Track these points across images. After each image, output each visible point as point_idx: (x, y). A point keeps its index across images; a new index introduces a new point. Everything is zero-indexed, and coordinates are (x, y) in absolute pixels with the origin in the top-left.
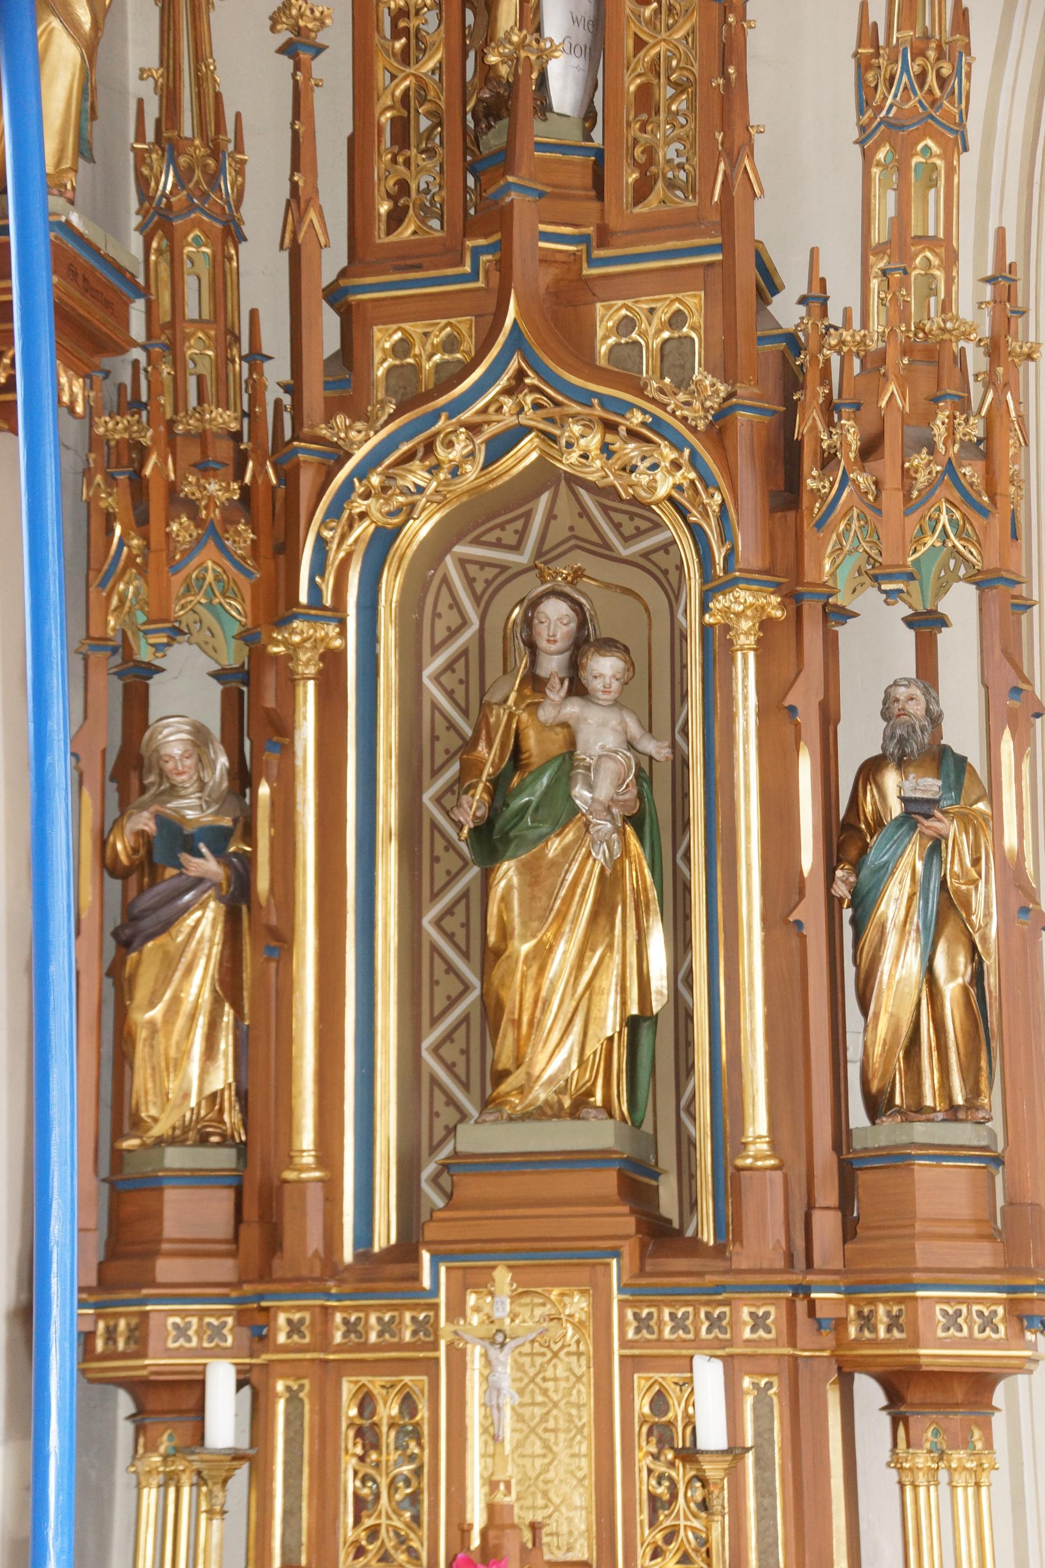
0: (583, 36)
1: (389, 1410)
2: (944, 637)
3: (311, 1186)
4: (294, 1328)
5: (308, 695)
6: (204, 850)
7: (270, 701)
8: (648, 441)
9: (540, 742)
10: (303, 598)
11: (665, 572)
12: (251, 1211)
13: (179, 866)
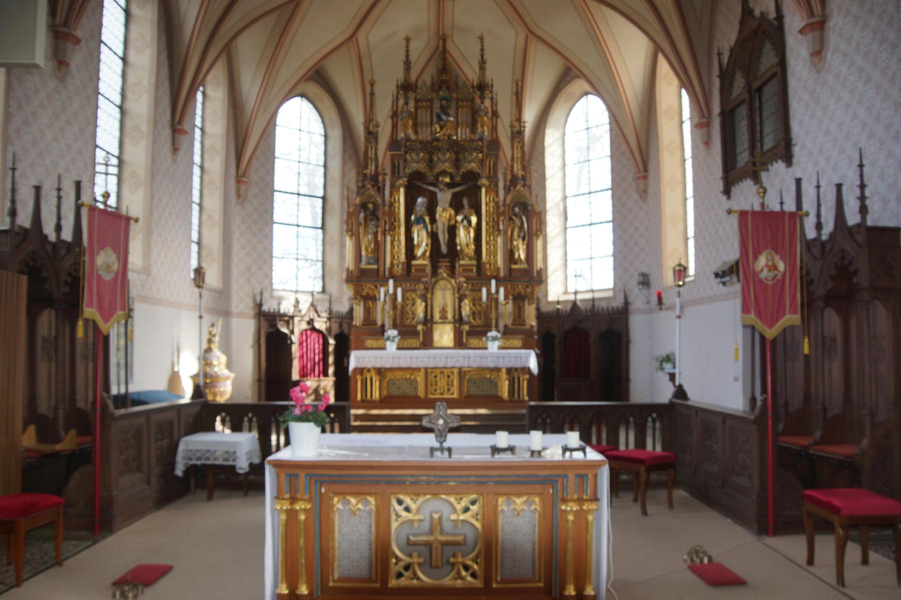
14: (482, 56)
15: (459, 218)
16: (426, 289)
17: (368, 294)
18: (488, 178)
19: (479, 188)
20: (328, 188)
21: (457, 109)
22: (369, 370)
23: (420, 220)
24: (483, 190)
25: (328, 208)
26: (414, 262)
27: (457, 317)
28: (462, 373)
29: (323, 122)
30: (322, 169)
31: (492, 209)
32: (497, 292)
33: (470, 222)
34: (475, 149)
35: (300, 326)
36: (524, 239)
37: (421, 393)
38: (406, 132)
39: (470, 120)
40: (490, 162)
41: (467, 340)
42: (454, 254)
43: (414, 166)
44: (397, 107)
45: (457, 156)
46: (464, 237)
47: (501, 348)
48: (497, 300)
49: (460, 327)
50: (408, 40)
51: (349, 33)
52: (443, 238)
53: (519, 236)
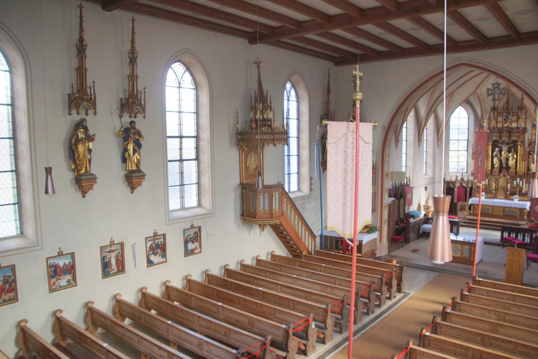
15: (510, 155)
16: (496, 180)
18: (521, 142)
19: (517, 146)
20: (469, 136)
21: (512, 115)
22: (475, 205)
23: (496, 156)
24: (519, 146)
25: (469, 143)
26: (494, 170)
27: (506, 189)
28: (504, 208)
29: (468, 114)
30: (467, 130)
32: (520, 182)
33: (513, 157)
34: (516, 133)
35: (457, 185)
37: (491, 213)
38: (493, 124)
40: (522, 136)
42: (508, 168)
43: (495, 138)
44: (490, 116)
45: (510, 135)
46: (511, 162)
47: (520, 200)
48: (519, 185)
51: (473, 91)
53: (532, 161)
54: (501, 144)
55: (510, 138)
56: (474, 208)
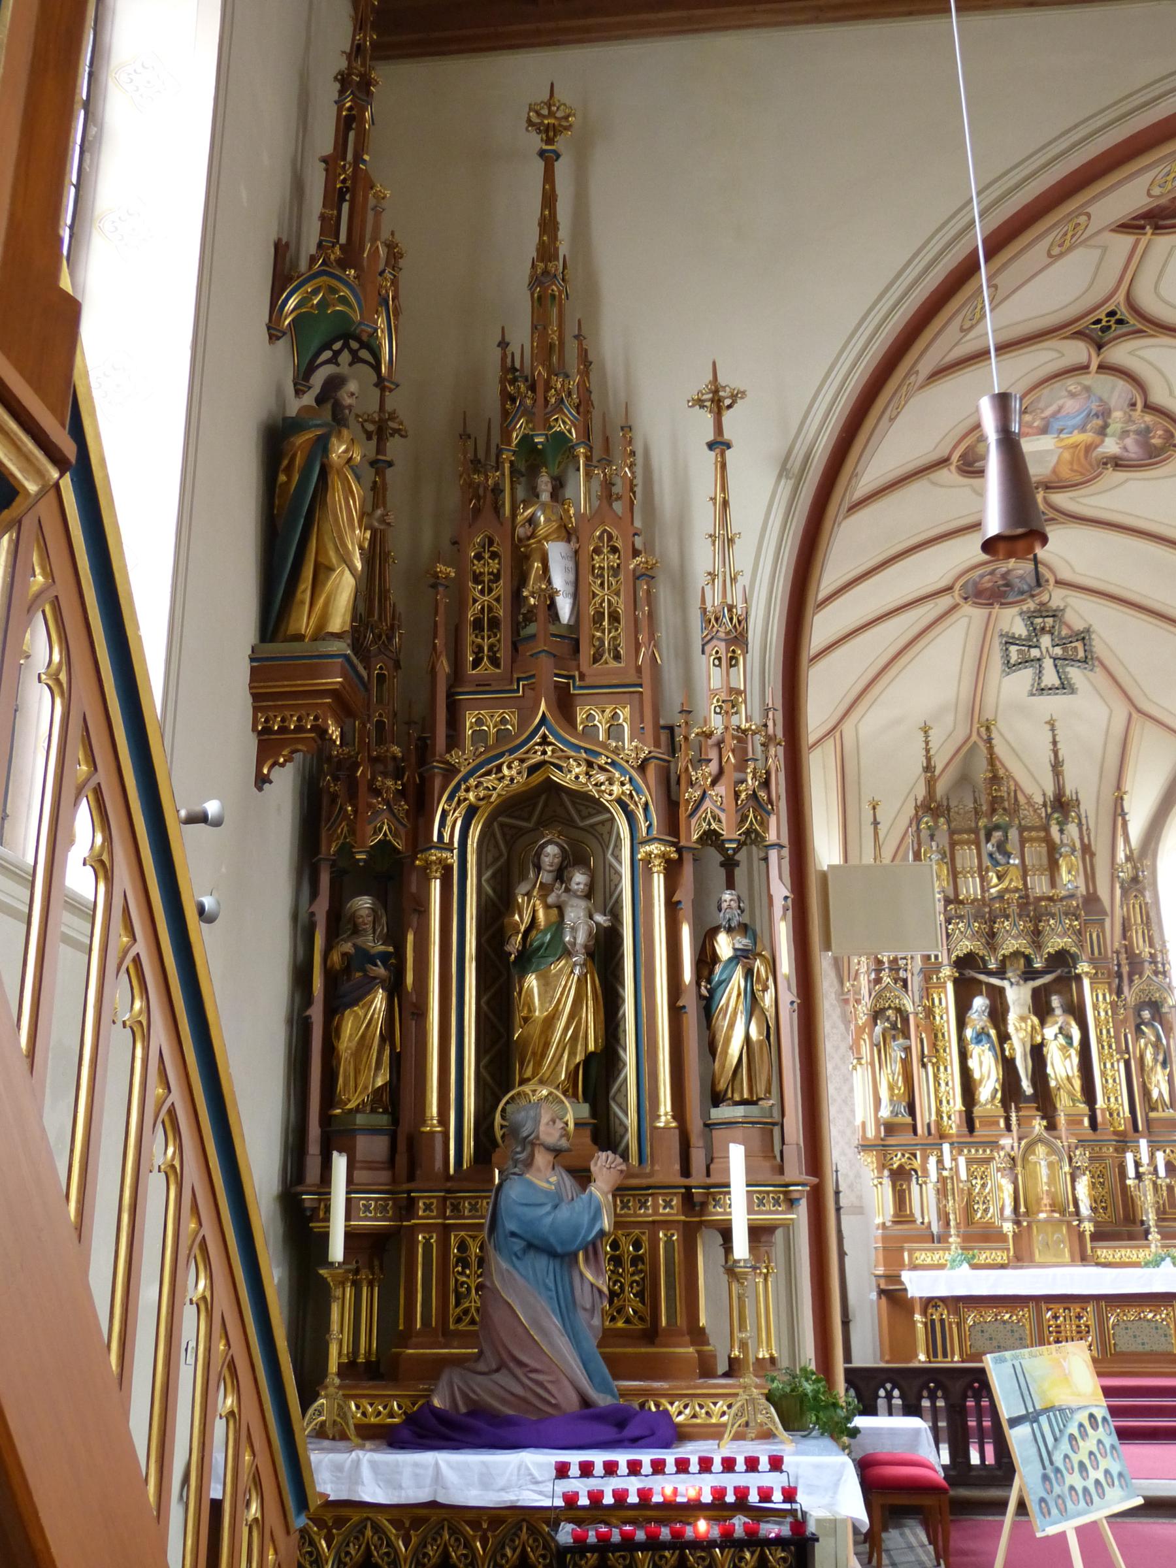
0: (571, 589)
1: (475, 1250)
2: (737, 871)
3: (437, 1135)
4: (428, 1207)
5: (436, 887)
6: (379, 963)
7: (414, 889)
8: (607, 770)
9: (546, 915)
10: (435, 839)
11: (602, 835)
12: (402, 1146)
13: (364, 971)
14: (1056, 753)
15: (1050, 1031)
17: (901, 1167)
19: (1078, 978)
23: (981, 1036)
24: (1086, 982)
26: (977, 1111)
31: (1103, 1014)
33: (1069, 1038)
34: (1066, 914)
36: (1164, 1064)
39: (1045, 861)
41: (1092, 1248)
43: (966, 946)
49: (1078, 1225)
50: (926, 731)
52: (1023, 1067)
53: (1155, 1060)
54: (1001, 973)
55: (1038, 946)
56: (930, 1326)
